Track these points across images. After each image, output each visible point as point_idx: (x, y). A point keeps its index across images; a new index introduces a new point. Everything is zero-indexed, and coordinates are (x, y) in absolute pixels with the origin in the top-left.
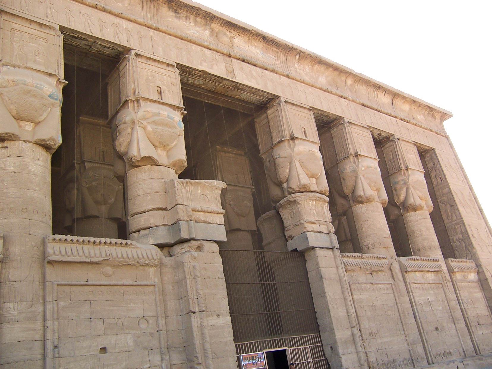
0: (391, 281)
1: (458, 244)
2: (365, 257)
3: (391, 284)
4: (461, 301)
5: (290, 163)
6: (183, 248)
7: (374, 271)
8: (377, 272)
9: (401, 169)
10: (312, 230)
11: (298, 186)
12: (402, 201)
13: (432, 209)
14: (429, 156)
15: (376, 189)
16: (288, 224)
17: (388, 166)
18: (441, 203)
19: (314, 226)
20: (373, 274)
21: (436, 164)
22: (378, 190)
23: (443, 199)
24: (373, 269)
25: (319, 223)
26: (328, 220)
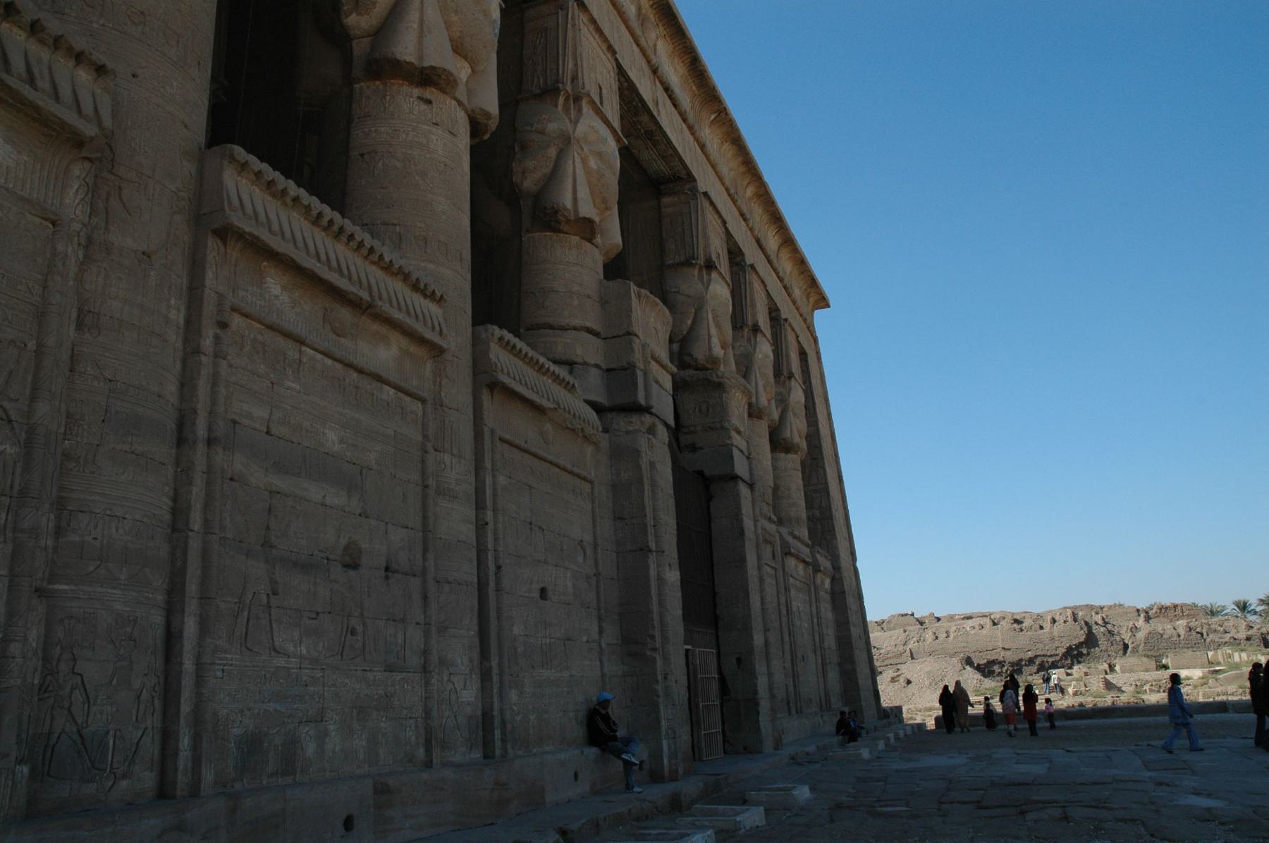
6: (631, 422)
11: (705, 356)
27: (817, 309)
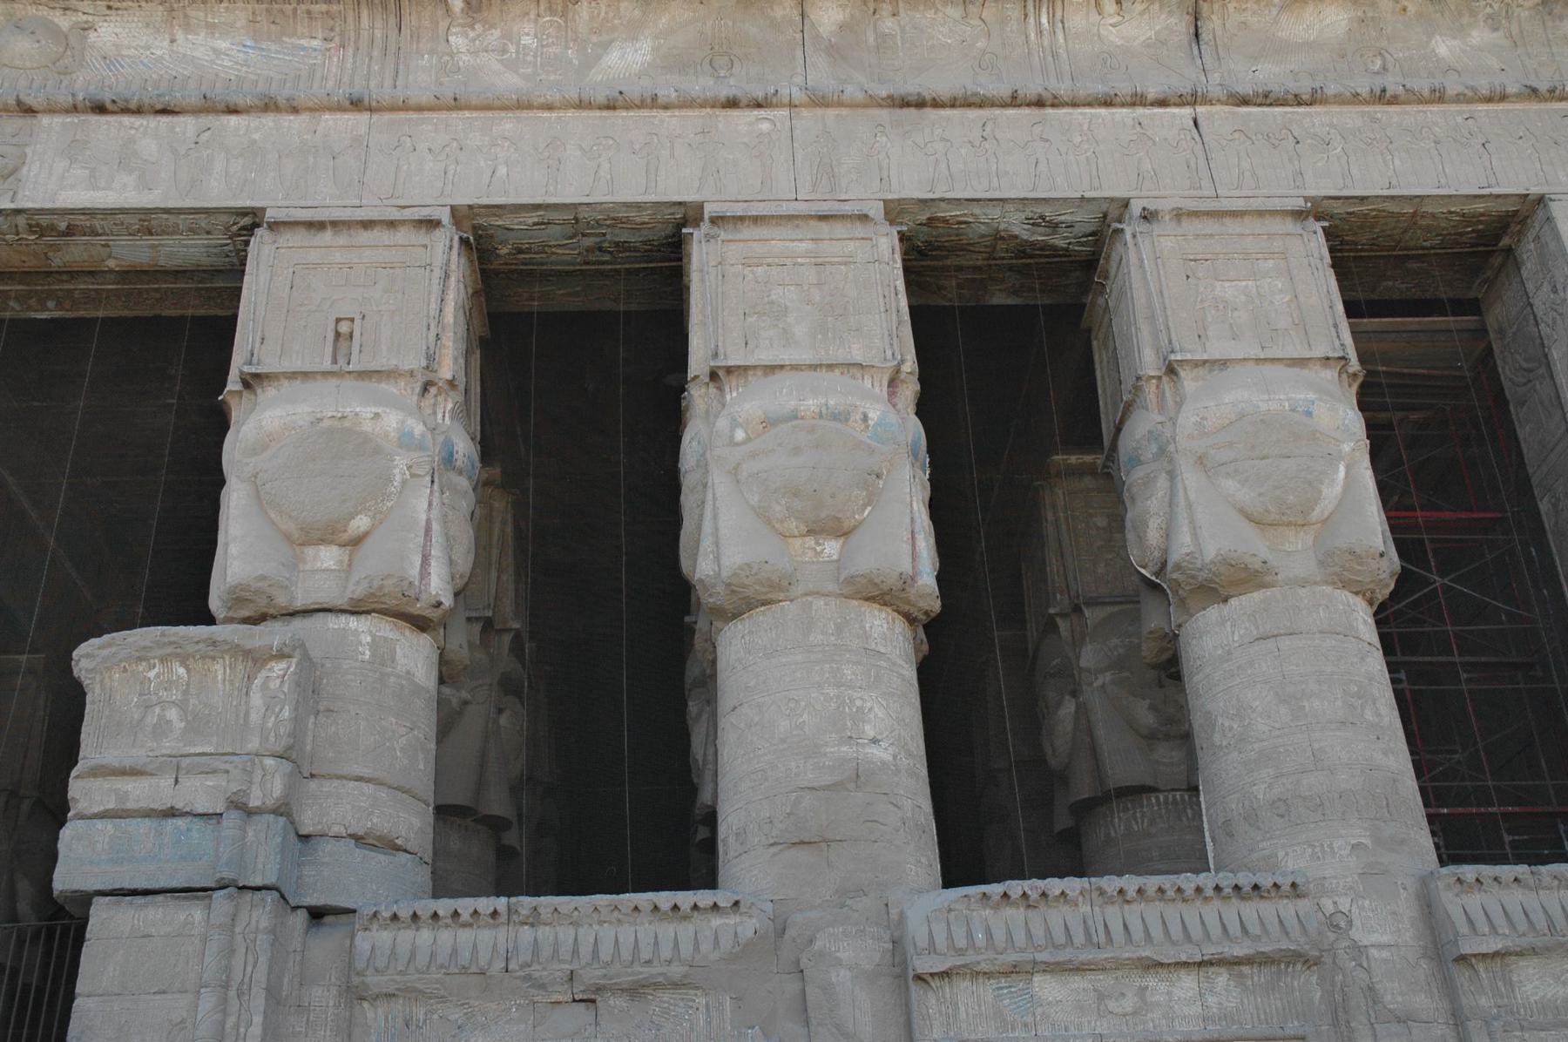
10: (111, 806)
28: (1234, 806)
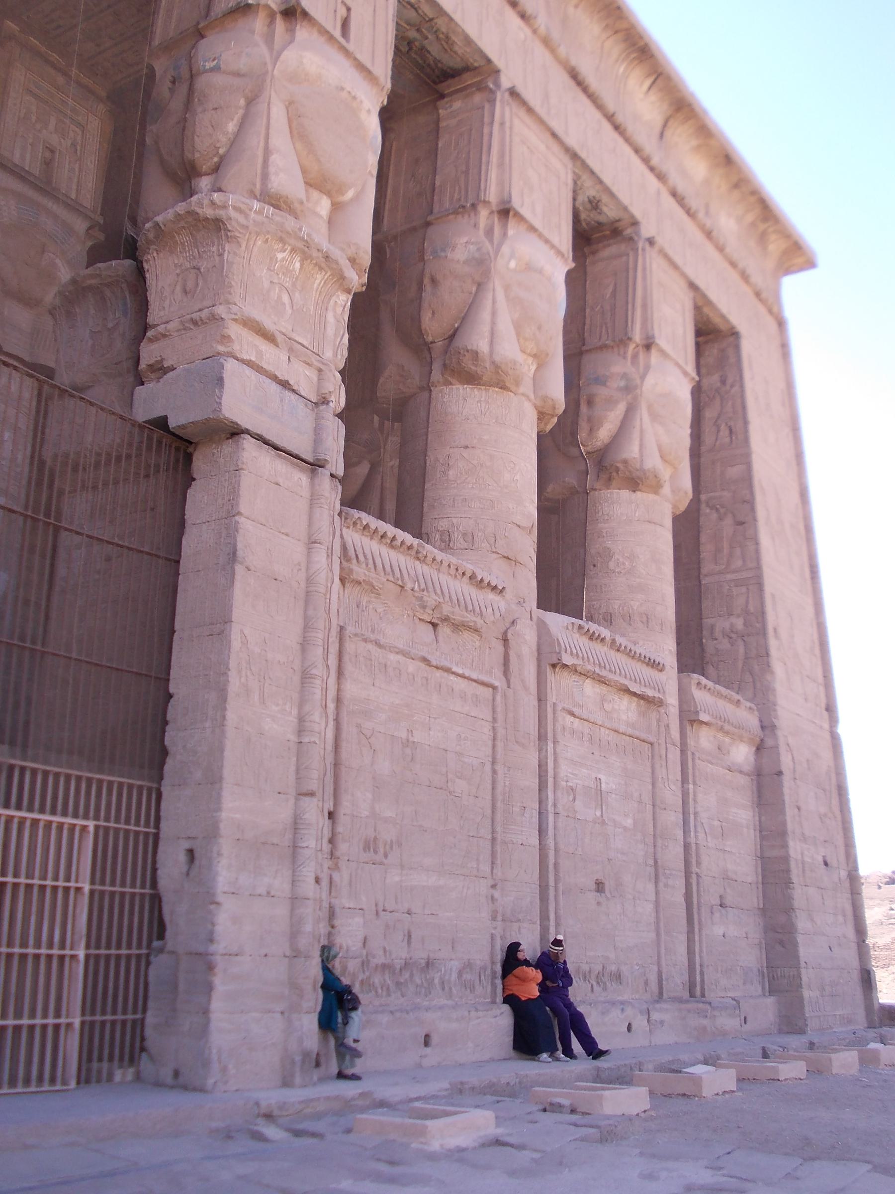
0: (498, 681)
1: (725, 644)
2: (429, 559)
3: (494, 688)
4: (692, 816)
5: (251, 101)
7: (446, 619)
8: (458, 627)
9: (630, 339)
10: (253, 359)
12: (599, 444)
13: (683, 506)
14: (715, 351)
15: (535, 351)
16: (162, 313)
17: (588, 321)
18: (708, 505)
19: (264, 346)
20: (439, 628)
21: (729, 381)
22: (541, 359)
23: (717, 494)
24: (446, 610)
25: (291, 350)
26: (328, 354)
27: (788, 271)
28: (616, 607)
